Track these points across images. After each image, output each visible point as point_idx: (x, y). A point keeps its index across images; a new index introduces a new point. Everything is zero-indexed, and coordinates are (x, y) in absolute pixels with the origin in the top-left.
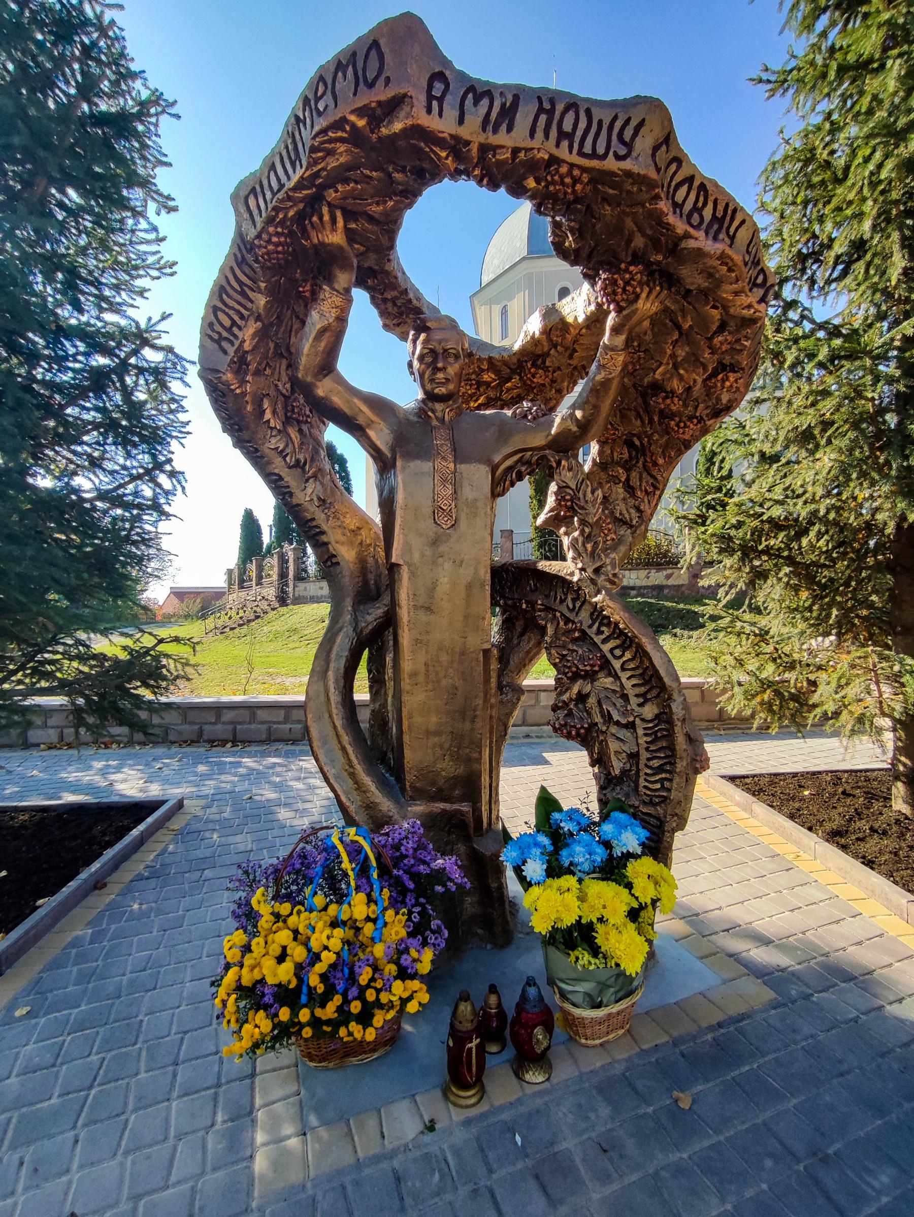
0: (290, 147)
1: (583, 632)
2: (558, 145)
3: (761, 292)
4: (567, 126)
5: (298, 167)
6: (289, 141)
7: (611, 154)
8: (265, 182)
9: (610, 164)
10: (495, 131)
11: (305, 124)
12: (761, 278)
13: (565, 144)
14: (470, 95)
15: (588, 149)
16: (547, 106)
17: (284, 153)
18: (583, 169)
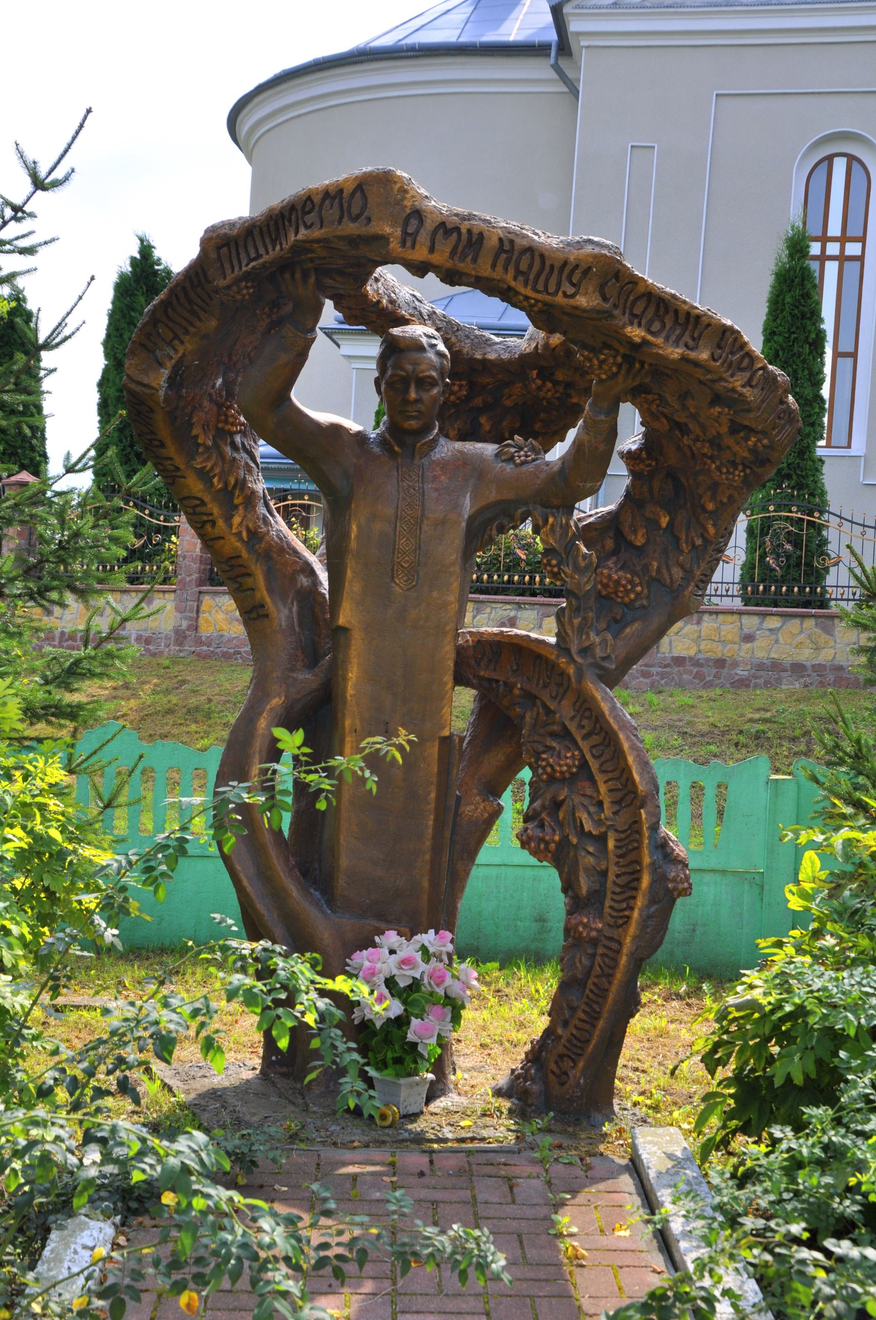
0: (272, 228)
1: (565, 728)
2: (515, 279)
3: (747, 374)
4: (523, 267)
5: (278, 248)
6: (272, 223)
7: (560, 293)
8: (241, 243)
9: (559, 299)
10: (463, 259)
11: (290, 220)
12: (746, 361)
13: (521, 278)
14: (441, 231)
15: (540, 287)
16: (507, 247)
17: (265, 229)
18: (537, 301)
